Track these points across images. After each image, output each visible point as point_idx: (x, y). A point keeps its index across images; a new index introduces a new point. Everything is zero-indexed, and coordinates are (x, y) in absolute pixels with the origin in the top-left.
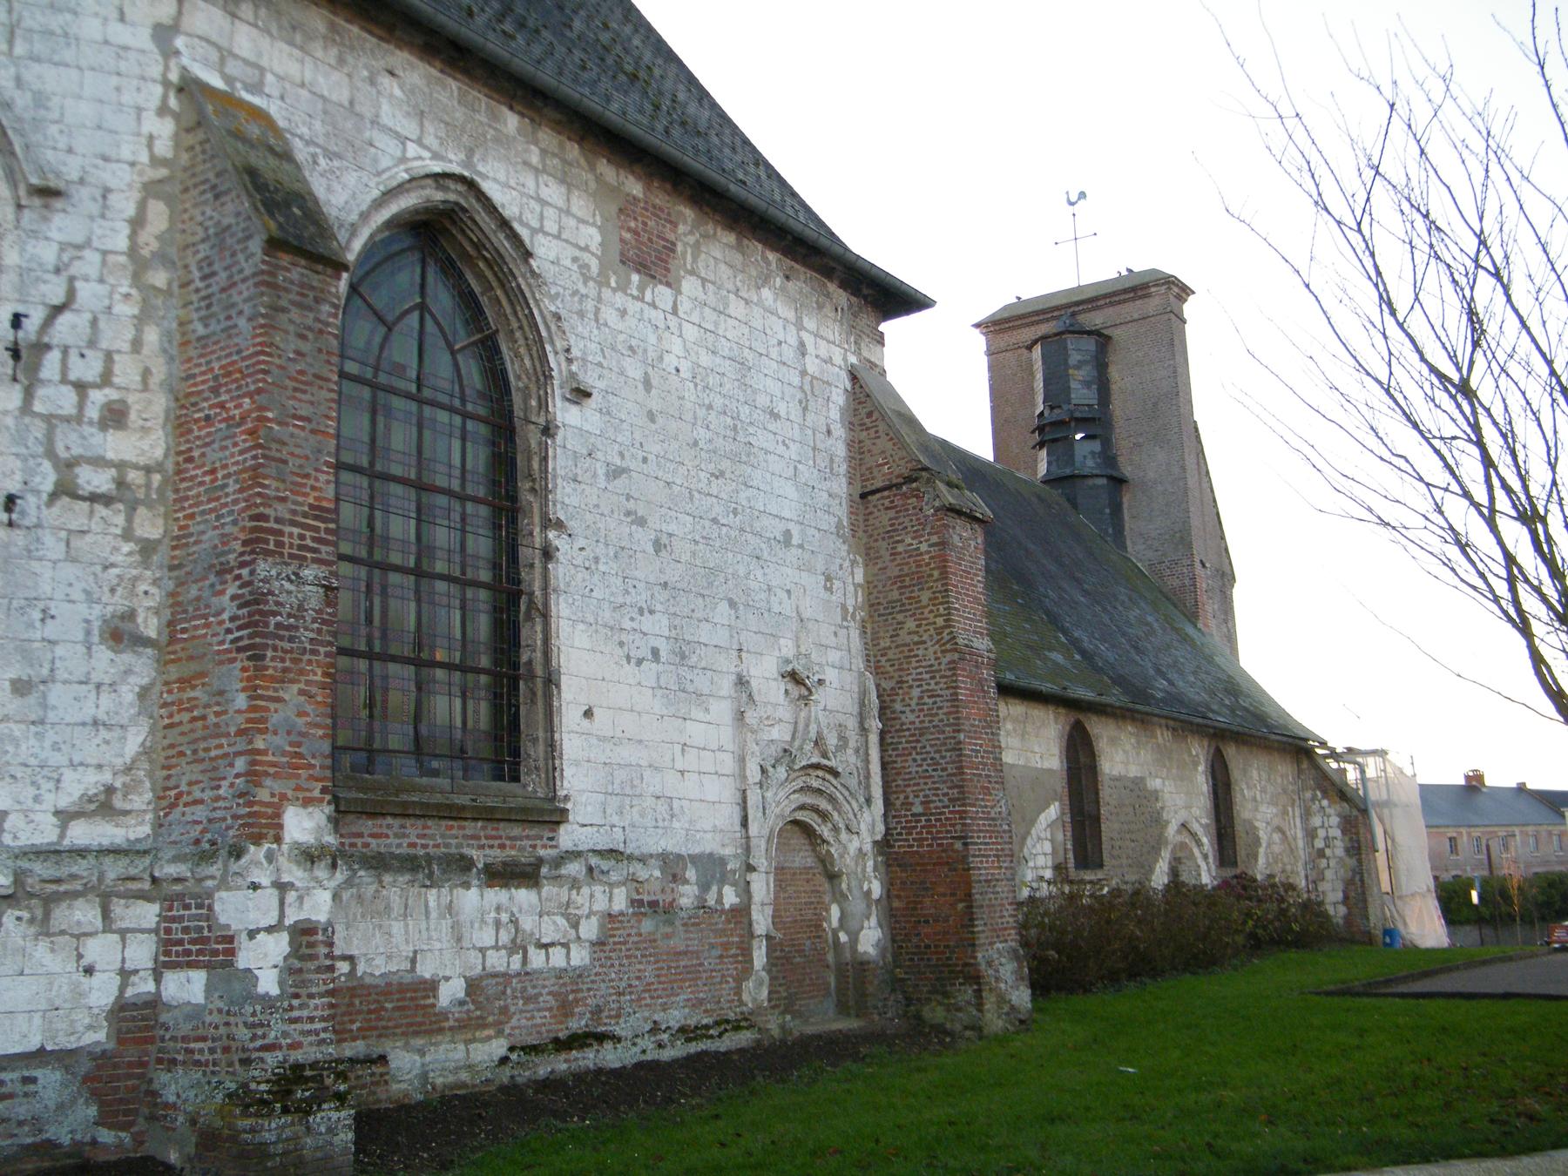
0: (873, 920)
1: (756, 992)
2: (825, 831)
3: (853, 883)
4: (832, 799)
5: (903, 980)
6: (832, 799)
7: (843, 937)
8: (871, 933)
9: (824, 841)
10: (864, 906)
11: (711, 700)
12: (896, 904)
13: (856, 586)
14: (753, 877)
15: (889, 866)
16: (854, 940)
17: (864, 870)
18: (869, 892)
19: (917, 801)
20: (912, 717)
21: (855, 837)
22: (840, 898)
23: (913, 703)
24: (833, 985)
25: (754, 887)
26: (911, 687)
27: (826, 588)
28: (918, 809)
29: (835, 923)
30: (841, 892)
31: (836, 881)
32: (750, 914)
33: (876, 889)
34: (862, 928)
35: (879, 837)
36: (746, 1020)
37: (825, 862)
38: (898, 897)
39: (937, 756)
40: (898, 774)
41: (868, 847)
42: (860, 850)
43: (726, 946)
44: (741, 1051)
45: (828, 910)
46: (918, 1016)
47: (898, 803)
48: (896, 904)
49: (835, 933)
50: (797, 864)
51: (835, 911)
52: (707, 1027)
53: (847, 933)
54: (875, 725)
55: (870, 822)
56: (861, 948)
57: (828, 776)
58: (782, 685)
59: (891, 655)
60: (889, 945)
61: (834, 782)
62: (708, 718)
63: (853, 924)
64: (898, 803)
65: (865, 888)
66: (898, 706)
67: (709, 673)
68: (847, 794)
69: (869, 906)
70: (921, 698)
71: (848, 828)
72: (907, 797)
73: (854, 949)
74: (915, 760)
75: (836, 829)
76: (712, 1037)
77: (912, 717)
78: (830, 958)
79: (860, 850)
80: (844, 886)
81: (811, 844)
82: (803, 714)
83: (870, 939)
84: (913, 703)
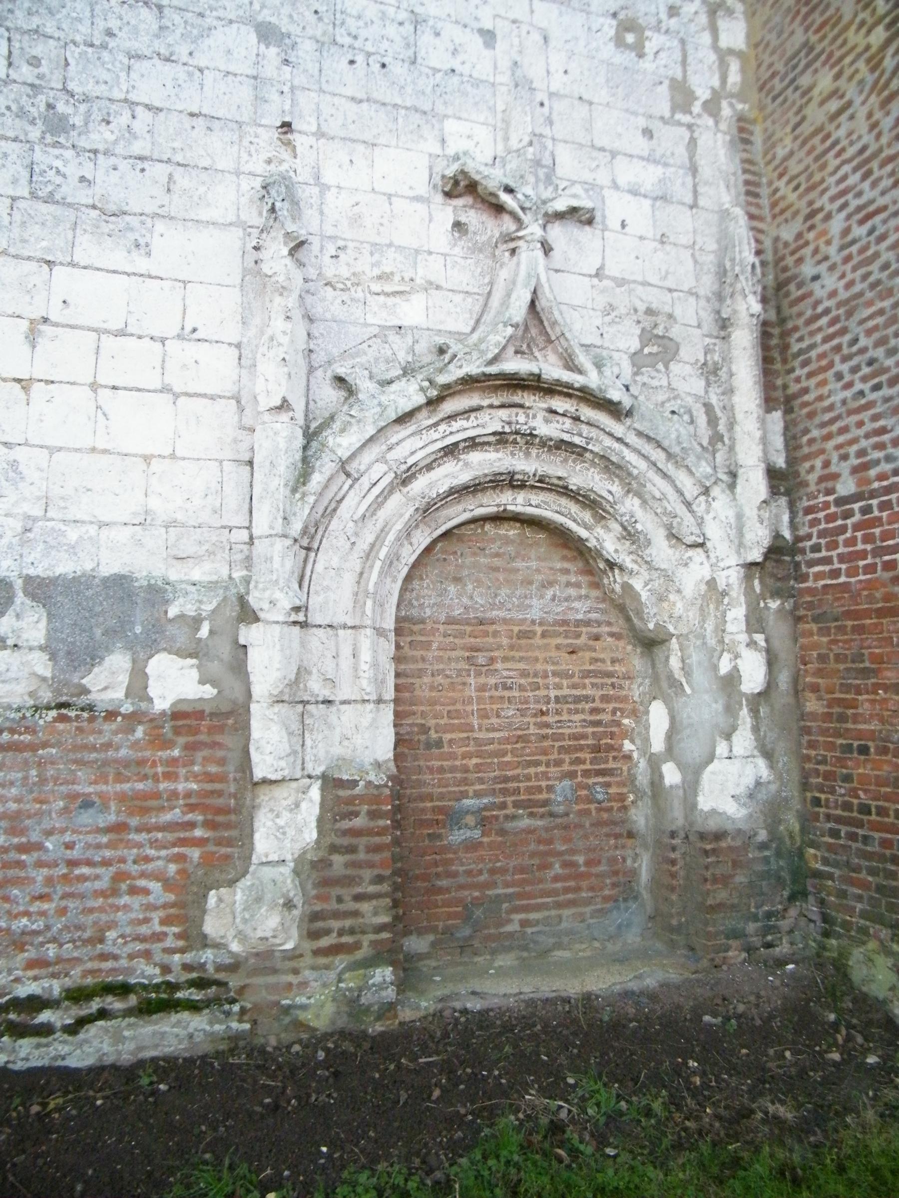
0: (744, 740)
1: (252, 916)
2: (607, 541)
3: (695, 658)
4: (611, 467)
5: (817, 874)
6: (611, 467)
7: (671, 775)
8: (733, 767)
9: (611, 565)
10: (719, 707)
11: (160, 226)
12: (812, 705)
13: (723, 55)
14: (249, 634)
15: (798, 619)
16: (692, 785)
17: (720, 629)
18: (731, 681)
19: (844, 468)
20: (830, 282)
21: (697, 555)
22: (667, 688)
23: (832, 250)
24: (644, 876)
25: (256, 660)
26: (828, 217)
27: (619, 42)
28: (846, 486)
29: (658, 744)
30: (670, 676)
31: (659, 652)
32: (245, 727)
33: (753, 674)
34: (711, 758)
35: (756, 555)
36: (201, 984)
37: (624, 607)
38: (815, 689)
39: (880, 353)
40: (811, 415)
41: (731, 578)
42: (711, 583)
43: (141, 804)
44: (165, 1067)
45: (639, 714)
46: (841, 968)
47: (812, 478)
48: (812, 705)
49: (655, 763)
50: (535, 613)
51: (658, 717)
52: (36, 1003)
53: (681, 766)
54: (748, 307)
55: (740, 521)
56: (704, 803)
57: (587, 413)
58: (446, 213)
59: (794, 167)
60: (792, 792)
61: (618, 429)
62: (142, 264)
63: (692, 749)
64: (812, 478)
65: (725, 666)
66: (808, 269)
67: (159, 171)
68: (658, 456)
69: (730, 710)
70: (846, 231)
71: (674, 537)
72: (827, 464)
73: (690, 805)
74: (839, 376)
75: (630, 535)
76: (46, 1030)
77: (830, 282)
78: (640, 817)
79: (711, 583)
80: (675, 663)
81: (589, 571)
82: (504, 274)
83: (731, 782)
84: (832, 250)
